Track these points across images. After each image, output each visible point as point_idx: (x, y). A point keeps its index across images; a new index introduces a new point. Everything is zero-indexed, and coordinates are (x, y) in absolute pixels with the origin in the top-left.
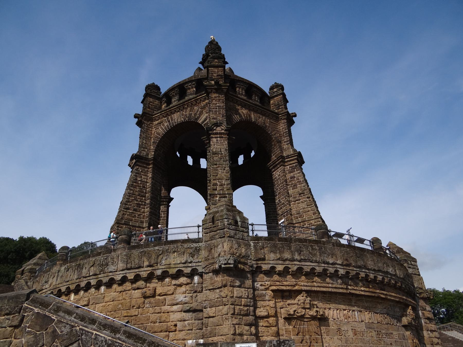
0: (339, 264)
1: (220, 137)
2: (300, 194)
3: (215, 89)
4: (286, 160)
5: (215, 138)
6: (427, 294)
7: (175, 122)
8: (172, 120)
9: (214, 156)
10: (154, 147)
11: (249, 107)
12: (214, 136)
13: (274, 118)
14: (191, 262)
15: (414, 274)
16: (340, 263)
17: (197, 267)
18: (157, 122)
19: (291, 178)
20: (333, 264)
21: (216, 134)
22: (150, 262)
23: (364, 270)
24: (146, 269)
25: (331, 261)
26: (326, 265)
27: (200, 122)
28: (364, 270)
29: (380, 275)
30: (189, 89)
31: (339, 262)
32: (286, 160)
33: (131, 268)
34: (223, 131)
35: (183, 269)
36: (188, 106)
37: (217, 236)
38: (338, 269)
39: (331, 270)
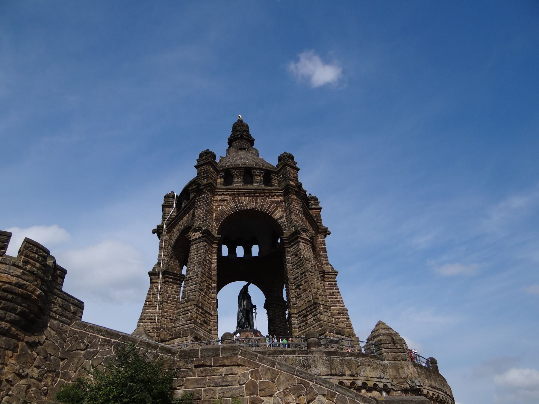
2: (339, 313)
3: (296, 191)
4: (326, 276)
5: (303, 243)
7: (244, 207)
8: (239, 203)
9: (306, 262)
10: (217, 225)
12: (302, 241)
14: (382, 378)
17: (387, 384)
18: (219, 198)
19: (331, 295)
21: (303, 239)
22: (352, 372)
24: (348, 378)
27: (276, 217)
30: (256, 176)
32: (326, 276)
33: (336, 375)
34: (308, 238)
35: (377, 383)
36: (260, 195)
37: (400, 358)
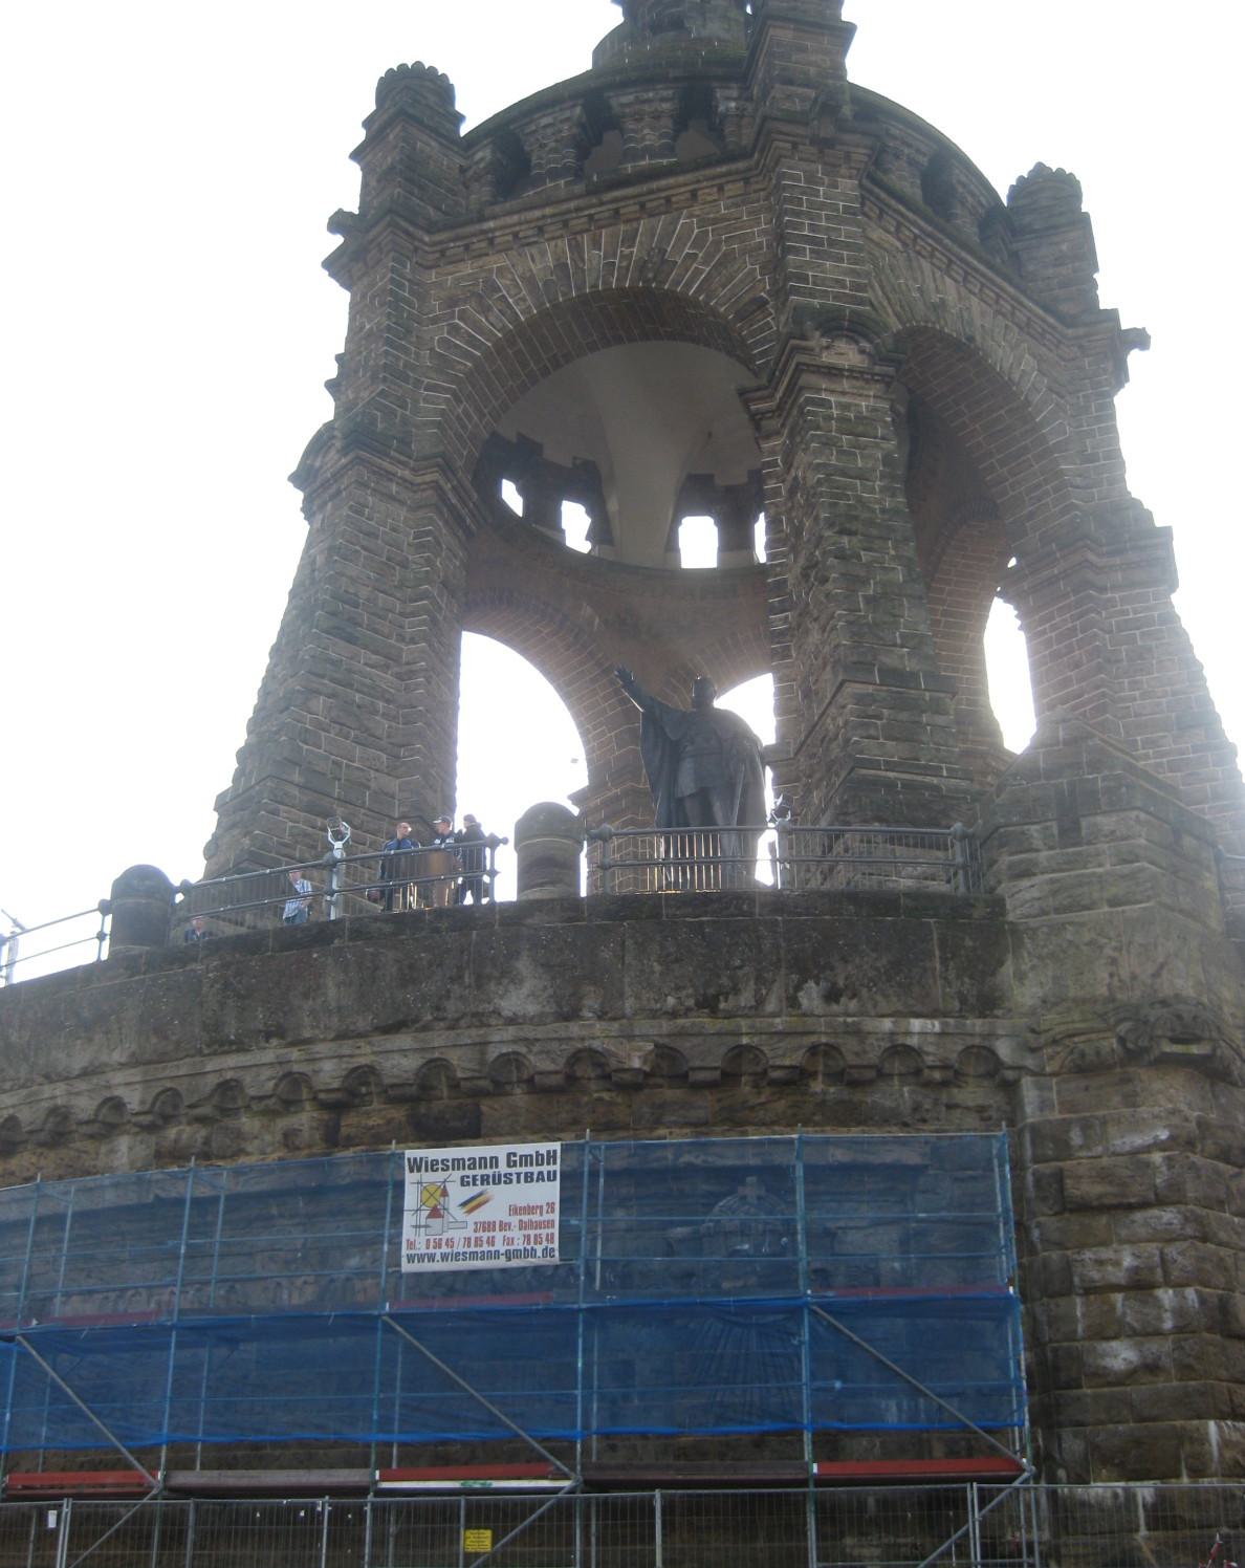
0: (122, 1066)
1: (332, 498)
6: (1123, 1028)
11: (565, 224)
13: (733, 189)
15: (1057, 911)
16: (123, 1060)
20: (85, 1074)
23: (268, 1056)
25: (79, 1063)
26: (60, 1089)
28: (268, 1056)
29: (403, 1052)
31: (117, 1056)
38: (118, 1092)
39: (85, 1106)
